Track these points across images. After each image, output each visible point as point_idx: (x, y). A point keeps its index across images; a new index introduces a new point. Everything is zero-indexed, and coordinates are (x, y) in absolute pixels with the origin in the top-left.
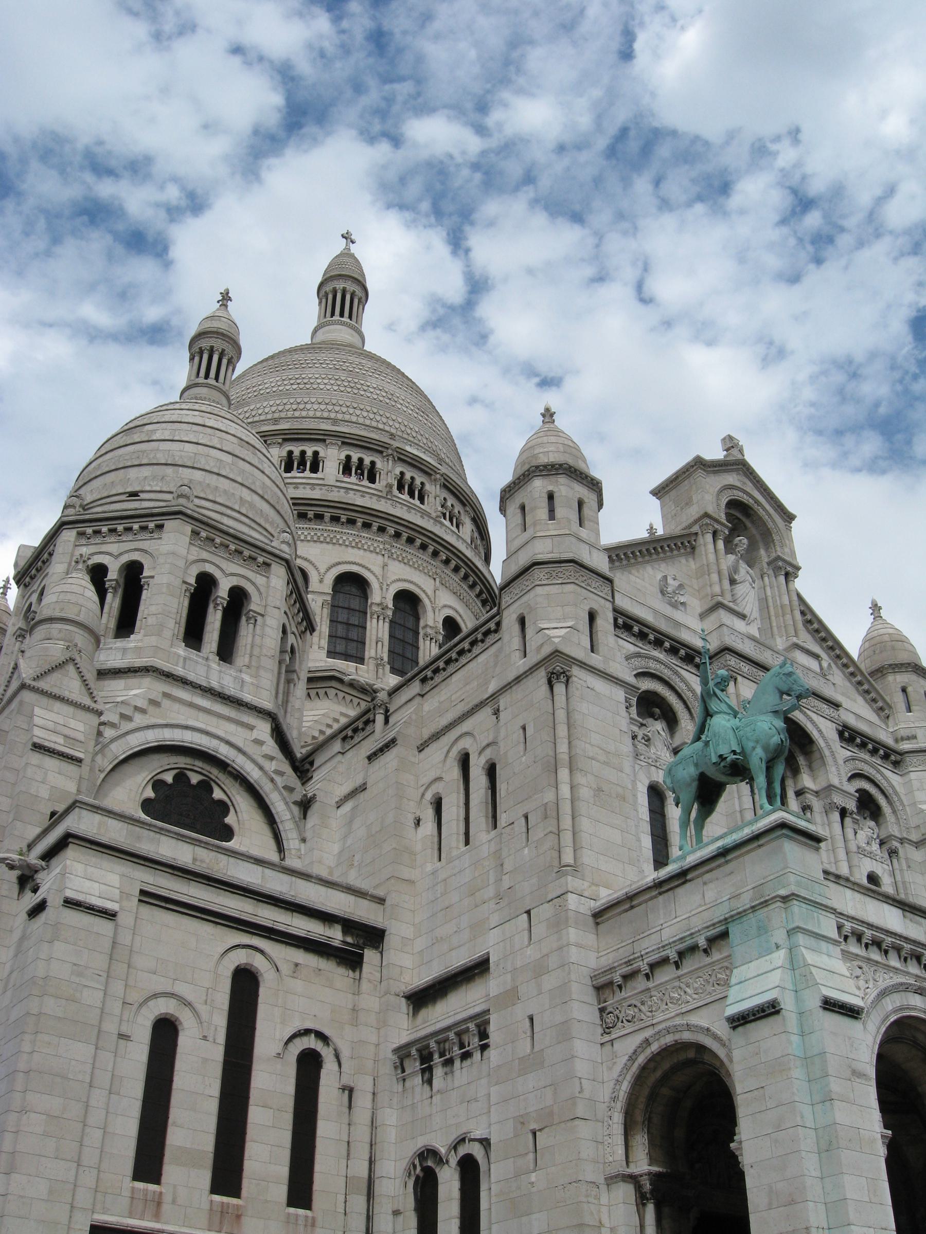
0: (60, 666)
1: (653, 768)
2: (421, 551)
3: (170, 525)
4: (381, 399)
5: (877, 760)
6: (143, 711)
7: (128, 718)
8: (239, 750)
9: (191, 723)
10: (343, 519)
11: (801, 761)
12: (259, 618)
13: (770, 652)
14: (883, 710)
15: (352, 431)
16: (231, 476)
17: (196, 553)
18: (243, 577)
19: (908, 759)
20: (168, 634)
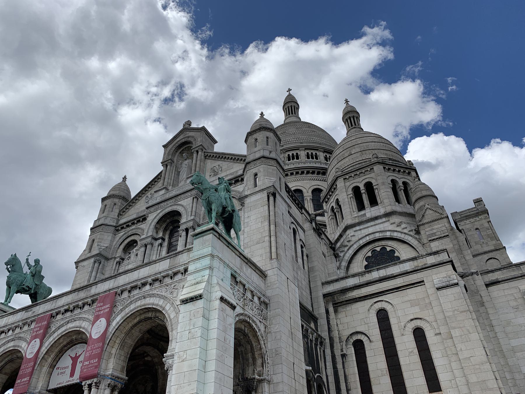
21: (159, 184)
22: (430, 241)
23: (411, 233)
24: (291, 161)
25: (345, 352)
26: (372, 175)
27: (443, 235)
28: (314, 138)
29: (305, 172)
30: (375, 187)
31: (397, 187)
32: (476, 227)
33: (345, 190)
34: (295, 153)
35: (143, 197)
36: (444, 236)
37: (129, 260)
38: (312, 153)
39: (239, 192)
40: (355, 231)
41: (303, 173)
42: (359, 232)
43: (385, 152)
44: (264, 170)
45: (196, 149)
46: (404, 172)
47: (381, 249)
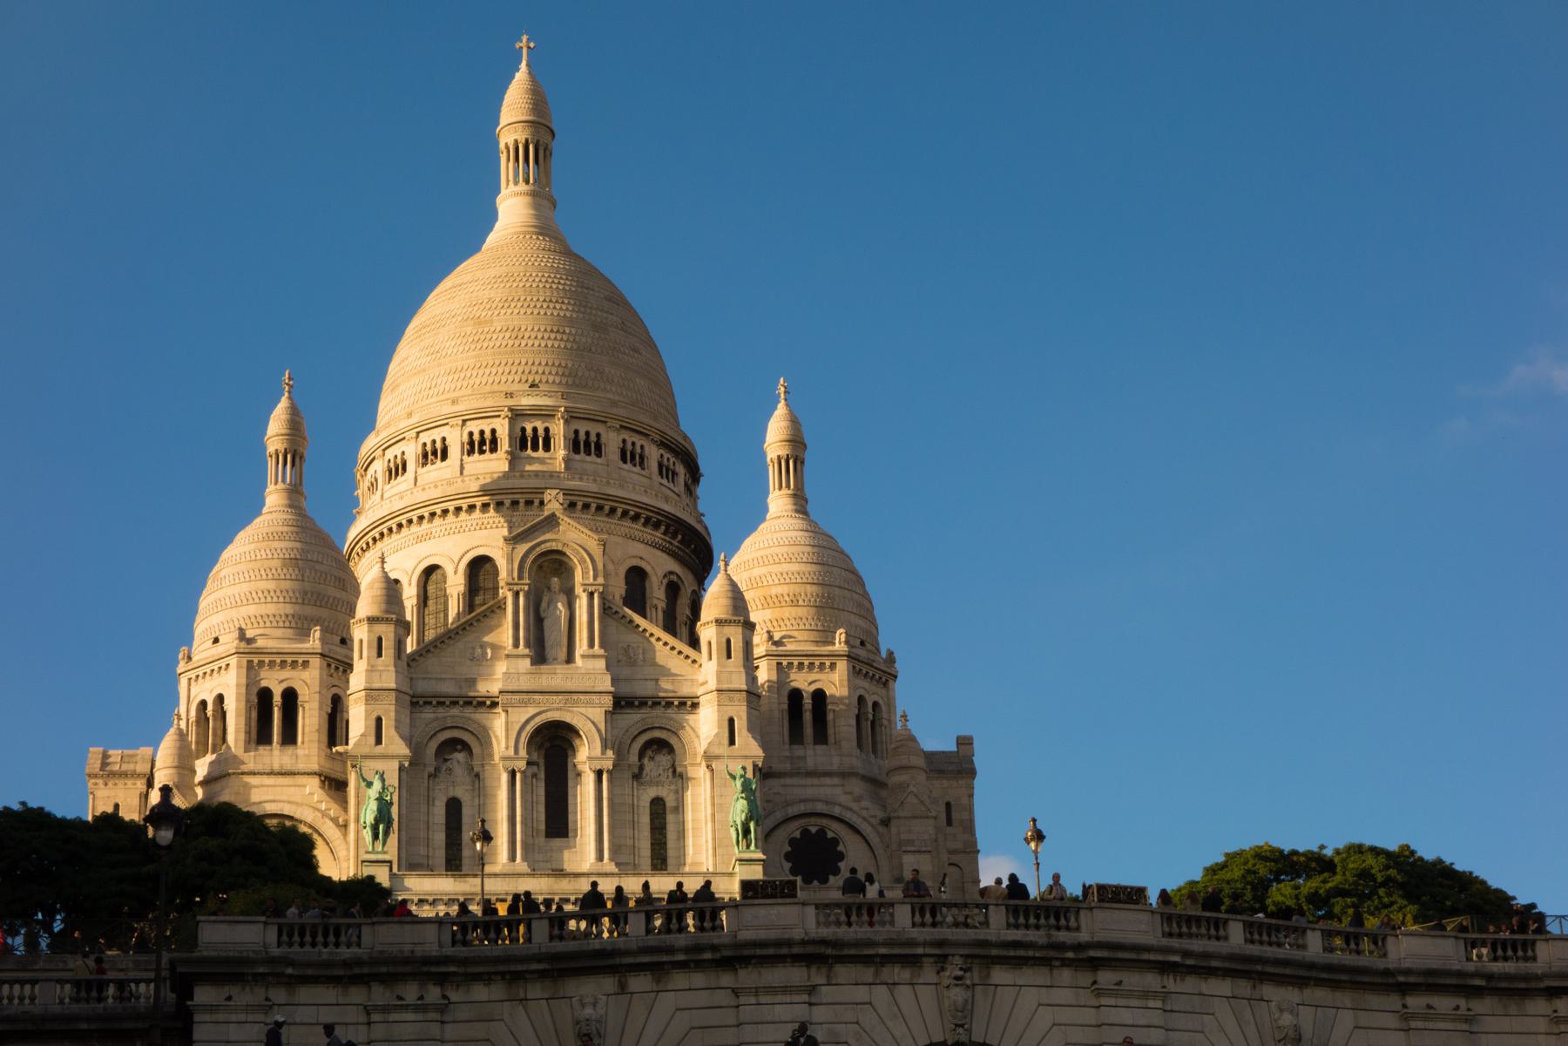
1: (451, 788)
4: (504, 343)
8: (297, 804)
11: (577, 742)
12: (307, 706)
13: (545, 677)
19: (702, 700)
20: (241, 744)
22: (905, 852)
23: (872, 820)
24: (582, 456)
27: (924, 849)
28: (637, 380)
29: (619, 512)
30: (829, 707)
31: (862, 711)
32: (947, 799)
34: (594, 429)
35: (457, 642)
36: (925, 852)
37: (450, 774)
38: (633, 444)
41: (613, 511)
44: (748, 718)
45: (591, 589)
46: (880, 678)
47: (817, 832)
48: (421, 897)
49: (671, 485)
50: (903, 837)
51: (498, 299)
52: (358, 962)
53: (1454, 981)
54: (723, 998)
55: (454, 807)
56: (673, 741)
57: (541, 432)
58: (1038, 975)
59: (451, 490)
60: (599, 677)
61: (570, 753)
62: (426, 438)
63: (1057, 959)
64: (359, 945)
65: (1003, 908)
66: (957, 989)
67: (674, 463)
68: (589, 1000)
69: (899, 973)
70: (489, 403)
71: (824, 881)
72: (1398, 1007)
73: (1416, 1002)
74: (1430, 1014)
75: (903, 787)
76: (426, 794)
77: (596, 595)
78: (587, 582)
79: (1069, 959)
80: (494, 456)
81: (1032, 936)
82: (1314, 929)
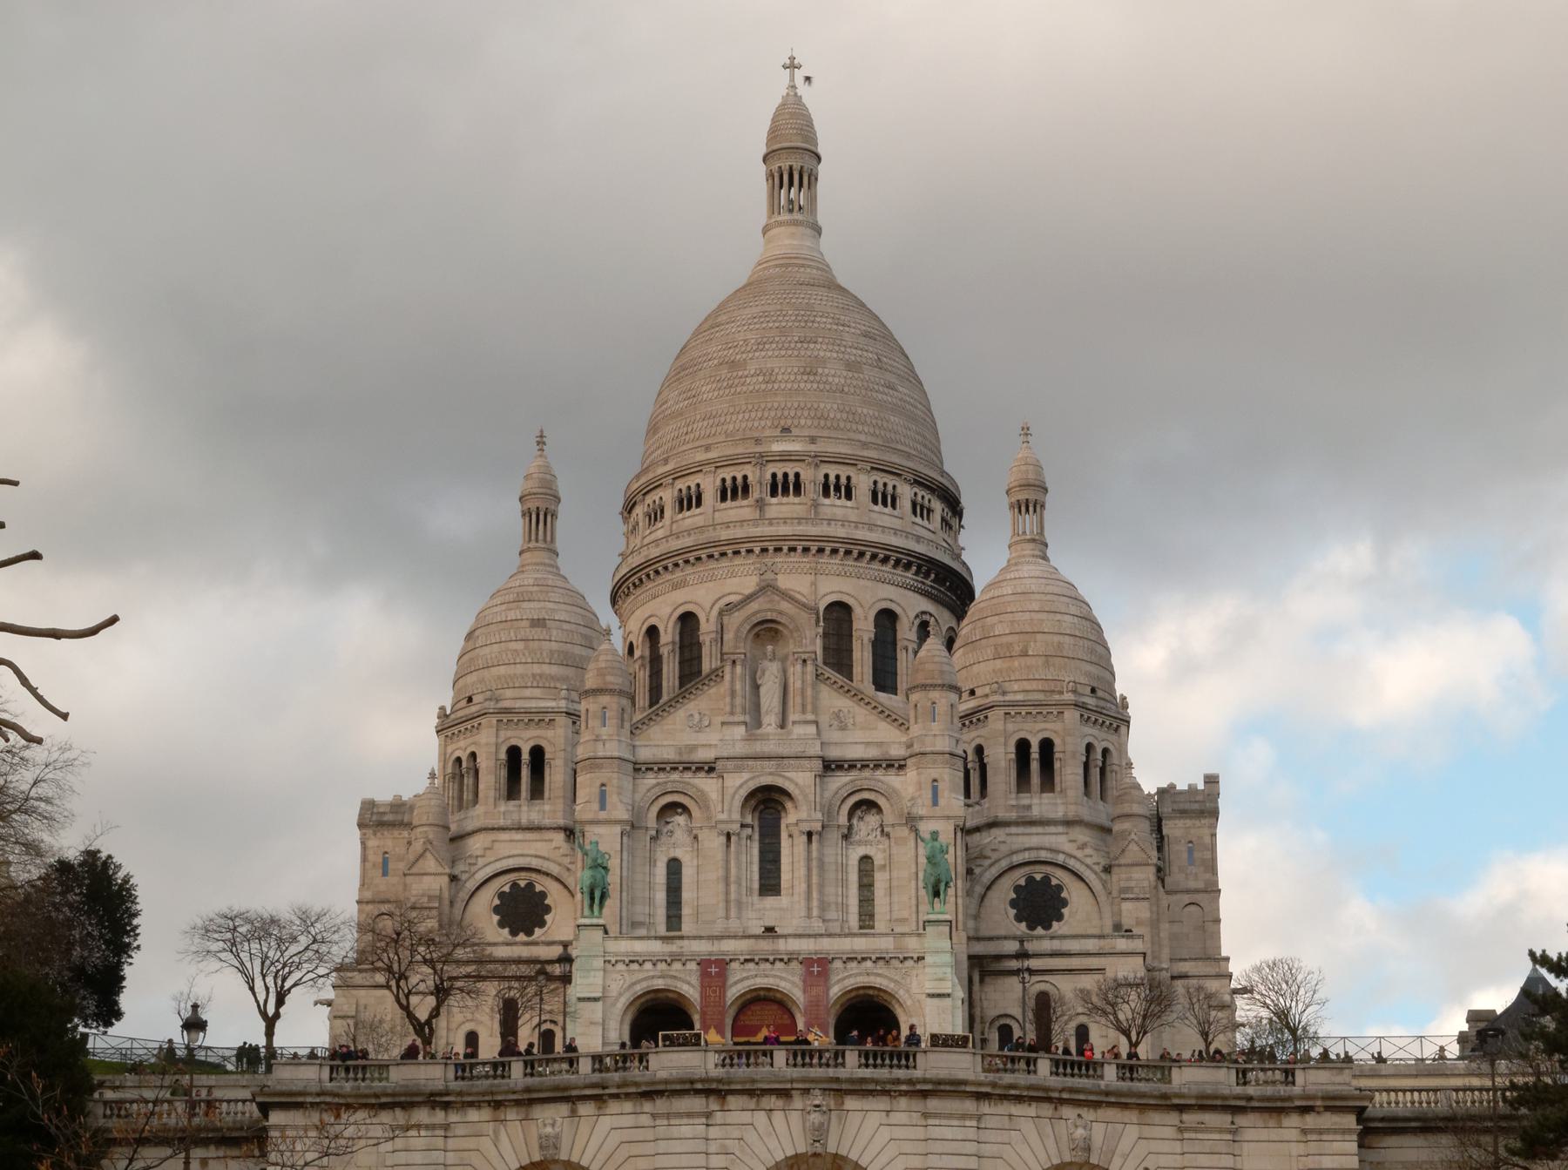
0: (422, 856)
2: (792, 554)
3: (484, 721)
5: (879, 773)
6: (483, 856)
7: (475, 864)
8: (544, 858)
9: (511, 853)
10: (716, 555)
11: (789, 805)
12: (552, 762)
13: (759, 742)
14: (903, 725)
15: (721, 454)
16: (523, 661)
17: (503, 734)
18: (537, 737)
19: (909, 762)
21: (713, 691)
23: (1097, 868)
24: (832, 500)
25: (986, 1036)
26: (1058, 726)
27: (1142, 896)
30: (1057, 756)
31: (1091, 758)
33: (1002, 740)
34: (844, 472)
38: (885, 485)
39: (895, 791)
40: (1008, 835)
41: (861, 554)
42: (1014, 839)
43: (1088, 667)
46: (1111, 724)
48: (632, 958)
49: (925, 523)
50: (1123, 884)
51: (753, 341)
52: (387, 1095)
53: (1219, 1102)
54: (645, 1120)
55: (674, 867)
56: (881, 801)
57: (791, 478)
58: (882, 1103)
59: (703, 538)
60: (810, 742)
61: (783, 814)
62: (681, 484)
63: (895, 1091)
64: (387, 1079)
65: (857, 1052)
66: (817, 1114)
67: (929, 501)
68: (551, 1122)
69: (772, 1102)
70: (740, 450)
71: (1047, 927)
72: (1177, 1122)
73: (1190, 1118)
74: (1201, 1128)
75: (1124, 834)
76: (648, 855)
77: (808, 662)
78: (800, 650)
79: (904, 1091)
80: (745, 502)
81: (883, 1073)
82: (1109, 1063)
